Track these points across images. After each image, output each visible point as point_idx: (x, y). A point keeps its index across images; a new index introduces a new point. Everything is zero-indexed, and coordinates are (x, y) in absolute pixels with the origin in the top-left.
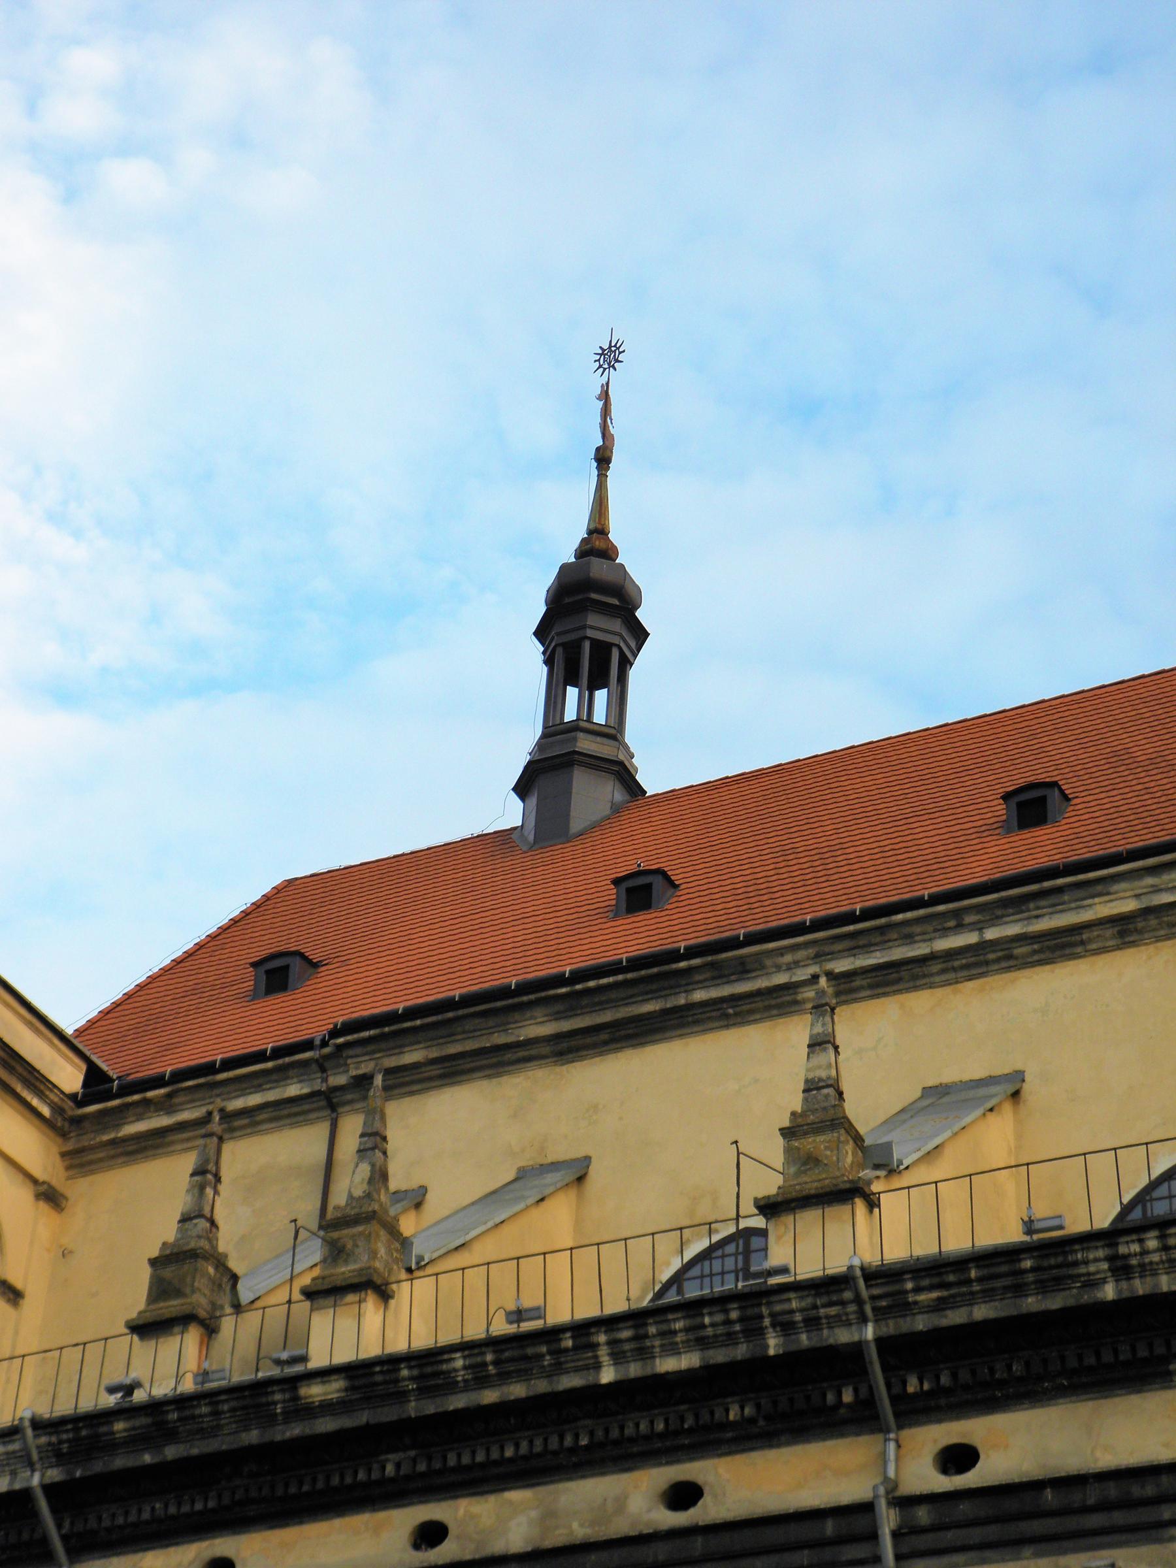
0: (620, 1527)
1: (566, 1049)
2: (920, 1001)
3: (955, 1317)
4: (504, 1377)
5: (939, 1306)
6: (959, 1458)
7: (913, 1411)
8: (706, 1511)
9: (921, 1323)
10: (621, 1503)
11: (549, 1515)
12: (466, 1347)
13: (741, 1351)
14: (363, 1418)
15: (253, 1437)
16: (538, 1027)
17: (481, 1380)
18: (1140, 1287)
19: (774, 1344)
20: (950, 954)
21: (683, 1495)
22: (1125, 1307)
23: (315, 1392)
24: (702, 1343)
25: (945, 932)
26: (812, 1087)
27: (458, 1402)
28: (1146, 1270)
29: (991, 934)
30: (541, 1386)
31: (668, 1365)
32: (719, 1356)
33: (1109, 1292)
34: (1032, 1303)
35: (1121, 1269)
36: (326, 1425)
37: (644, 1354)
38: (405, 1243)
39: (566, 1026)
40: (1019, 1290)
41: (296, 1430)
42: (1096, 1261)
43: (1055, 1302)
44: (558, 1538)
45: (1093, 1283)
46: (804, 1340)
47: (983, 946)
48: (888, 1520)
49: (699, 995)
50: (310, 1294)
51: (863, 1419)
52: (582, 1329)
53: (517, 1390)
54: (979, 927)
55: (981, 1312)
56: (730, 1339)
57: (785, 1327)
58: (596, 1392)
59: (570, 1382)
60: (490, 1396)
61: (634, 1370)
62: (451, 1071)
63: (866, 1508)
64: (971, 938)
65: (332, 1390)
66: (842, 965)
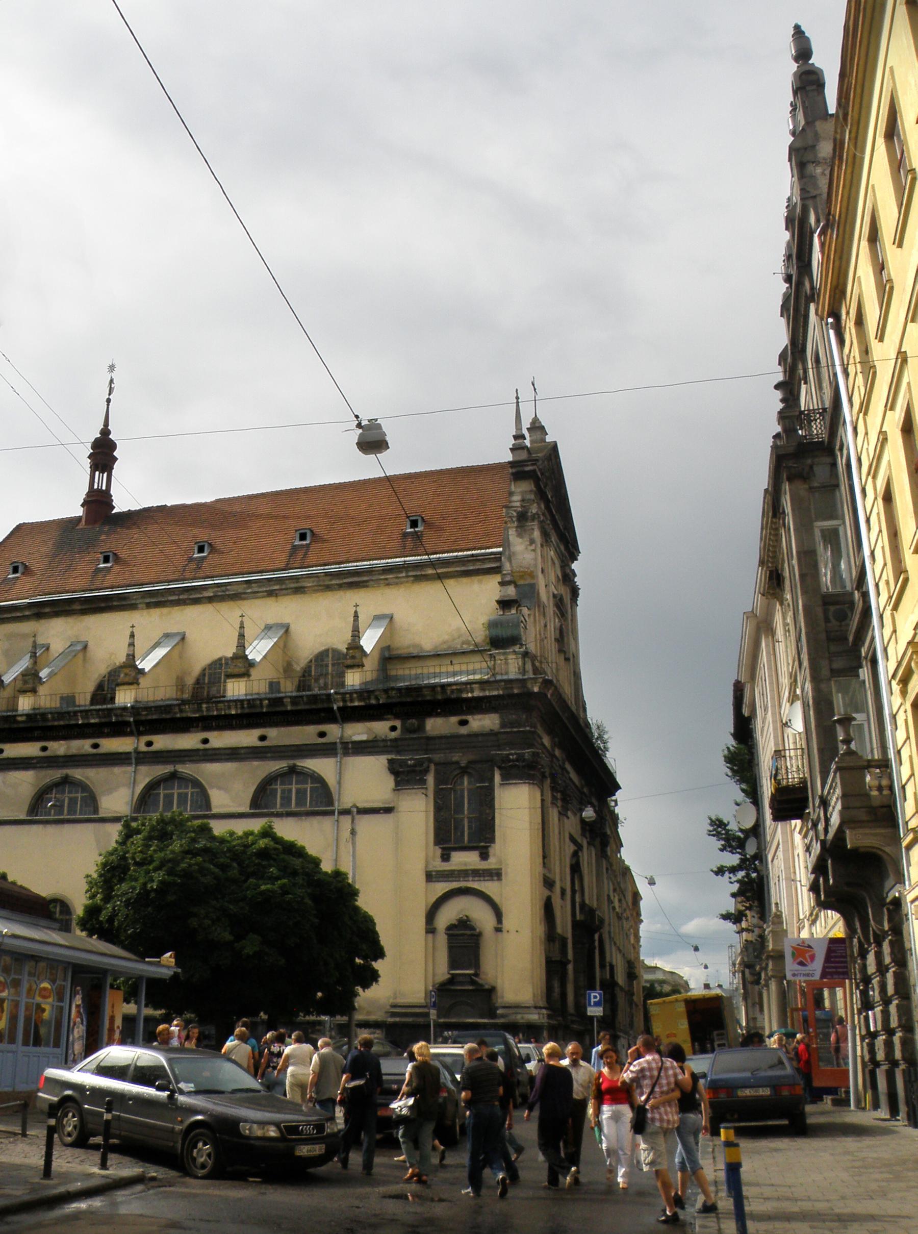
0: (83, 752)
1: (84, 612)
2: (165, 610)
3: (150, 717)
4: (59, 720)
5: (147, 715)
6: (149, 744)
7: (140, 734)
8: (101, 750)
9: (143, 718)
10: (83, 746)
11: (68, 748)
12: (51, 713)
13: (107, 720)
14: (29, 725)
15: (6, 726)
16: (77, 607)
17: (54, 719)
18: (184, 715)
19: (114, 719)
20: (172, 601)
21: (96, 746)
22: (182, 719)
23: (19, 719)
24: (99, 717)
25: (171, 595)
26: (128, 655)
27: (50, 724)
28: (186, 712)
29: (181, 597)
30: (67, 722)
31: (92, 721)
32: (103, 720)
33: (178, 715)
34: (164, 716)
35: (181, 711)
36: (21, 725)
37: (88, 718)
38: (41, 678)
39: (84, 607)
40: (162, 713)
41: (15, 726)
42: (177, 709)
43: (168, 716)
44: (70, 753)
45: (176, 713)
46: (120, 719)
47: (179, 600)
48: (133, 755)
49: (115, 603)
50: (19, 691)
51: (131, 734)
52: (75, 713)
53: (62, 723)
54: (179, 595)
55: (154, 717)
56: (105, 717)
57: (116, 716)
58: (77, 725)
59: (73, 722)
60: (56, 723)
61: (86, 721)
62: (56, 614)
63: (129, 753)
64: (177, 598)
65: (24, 718)
66: (148, 600)
